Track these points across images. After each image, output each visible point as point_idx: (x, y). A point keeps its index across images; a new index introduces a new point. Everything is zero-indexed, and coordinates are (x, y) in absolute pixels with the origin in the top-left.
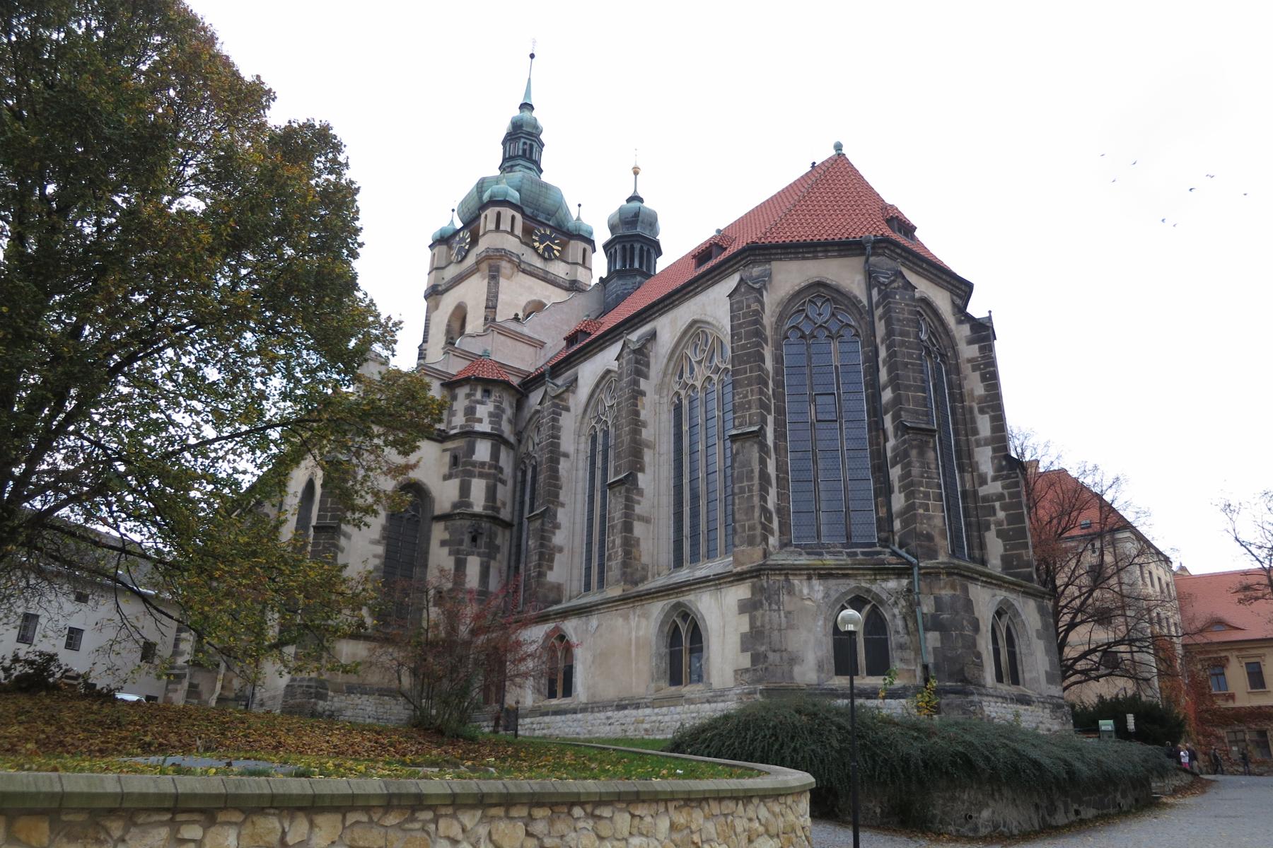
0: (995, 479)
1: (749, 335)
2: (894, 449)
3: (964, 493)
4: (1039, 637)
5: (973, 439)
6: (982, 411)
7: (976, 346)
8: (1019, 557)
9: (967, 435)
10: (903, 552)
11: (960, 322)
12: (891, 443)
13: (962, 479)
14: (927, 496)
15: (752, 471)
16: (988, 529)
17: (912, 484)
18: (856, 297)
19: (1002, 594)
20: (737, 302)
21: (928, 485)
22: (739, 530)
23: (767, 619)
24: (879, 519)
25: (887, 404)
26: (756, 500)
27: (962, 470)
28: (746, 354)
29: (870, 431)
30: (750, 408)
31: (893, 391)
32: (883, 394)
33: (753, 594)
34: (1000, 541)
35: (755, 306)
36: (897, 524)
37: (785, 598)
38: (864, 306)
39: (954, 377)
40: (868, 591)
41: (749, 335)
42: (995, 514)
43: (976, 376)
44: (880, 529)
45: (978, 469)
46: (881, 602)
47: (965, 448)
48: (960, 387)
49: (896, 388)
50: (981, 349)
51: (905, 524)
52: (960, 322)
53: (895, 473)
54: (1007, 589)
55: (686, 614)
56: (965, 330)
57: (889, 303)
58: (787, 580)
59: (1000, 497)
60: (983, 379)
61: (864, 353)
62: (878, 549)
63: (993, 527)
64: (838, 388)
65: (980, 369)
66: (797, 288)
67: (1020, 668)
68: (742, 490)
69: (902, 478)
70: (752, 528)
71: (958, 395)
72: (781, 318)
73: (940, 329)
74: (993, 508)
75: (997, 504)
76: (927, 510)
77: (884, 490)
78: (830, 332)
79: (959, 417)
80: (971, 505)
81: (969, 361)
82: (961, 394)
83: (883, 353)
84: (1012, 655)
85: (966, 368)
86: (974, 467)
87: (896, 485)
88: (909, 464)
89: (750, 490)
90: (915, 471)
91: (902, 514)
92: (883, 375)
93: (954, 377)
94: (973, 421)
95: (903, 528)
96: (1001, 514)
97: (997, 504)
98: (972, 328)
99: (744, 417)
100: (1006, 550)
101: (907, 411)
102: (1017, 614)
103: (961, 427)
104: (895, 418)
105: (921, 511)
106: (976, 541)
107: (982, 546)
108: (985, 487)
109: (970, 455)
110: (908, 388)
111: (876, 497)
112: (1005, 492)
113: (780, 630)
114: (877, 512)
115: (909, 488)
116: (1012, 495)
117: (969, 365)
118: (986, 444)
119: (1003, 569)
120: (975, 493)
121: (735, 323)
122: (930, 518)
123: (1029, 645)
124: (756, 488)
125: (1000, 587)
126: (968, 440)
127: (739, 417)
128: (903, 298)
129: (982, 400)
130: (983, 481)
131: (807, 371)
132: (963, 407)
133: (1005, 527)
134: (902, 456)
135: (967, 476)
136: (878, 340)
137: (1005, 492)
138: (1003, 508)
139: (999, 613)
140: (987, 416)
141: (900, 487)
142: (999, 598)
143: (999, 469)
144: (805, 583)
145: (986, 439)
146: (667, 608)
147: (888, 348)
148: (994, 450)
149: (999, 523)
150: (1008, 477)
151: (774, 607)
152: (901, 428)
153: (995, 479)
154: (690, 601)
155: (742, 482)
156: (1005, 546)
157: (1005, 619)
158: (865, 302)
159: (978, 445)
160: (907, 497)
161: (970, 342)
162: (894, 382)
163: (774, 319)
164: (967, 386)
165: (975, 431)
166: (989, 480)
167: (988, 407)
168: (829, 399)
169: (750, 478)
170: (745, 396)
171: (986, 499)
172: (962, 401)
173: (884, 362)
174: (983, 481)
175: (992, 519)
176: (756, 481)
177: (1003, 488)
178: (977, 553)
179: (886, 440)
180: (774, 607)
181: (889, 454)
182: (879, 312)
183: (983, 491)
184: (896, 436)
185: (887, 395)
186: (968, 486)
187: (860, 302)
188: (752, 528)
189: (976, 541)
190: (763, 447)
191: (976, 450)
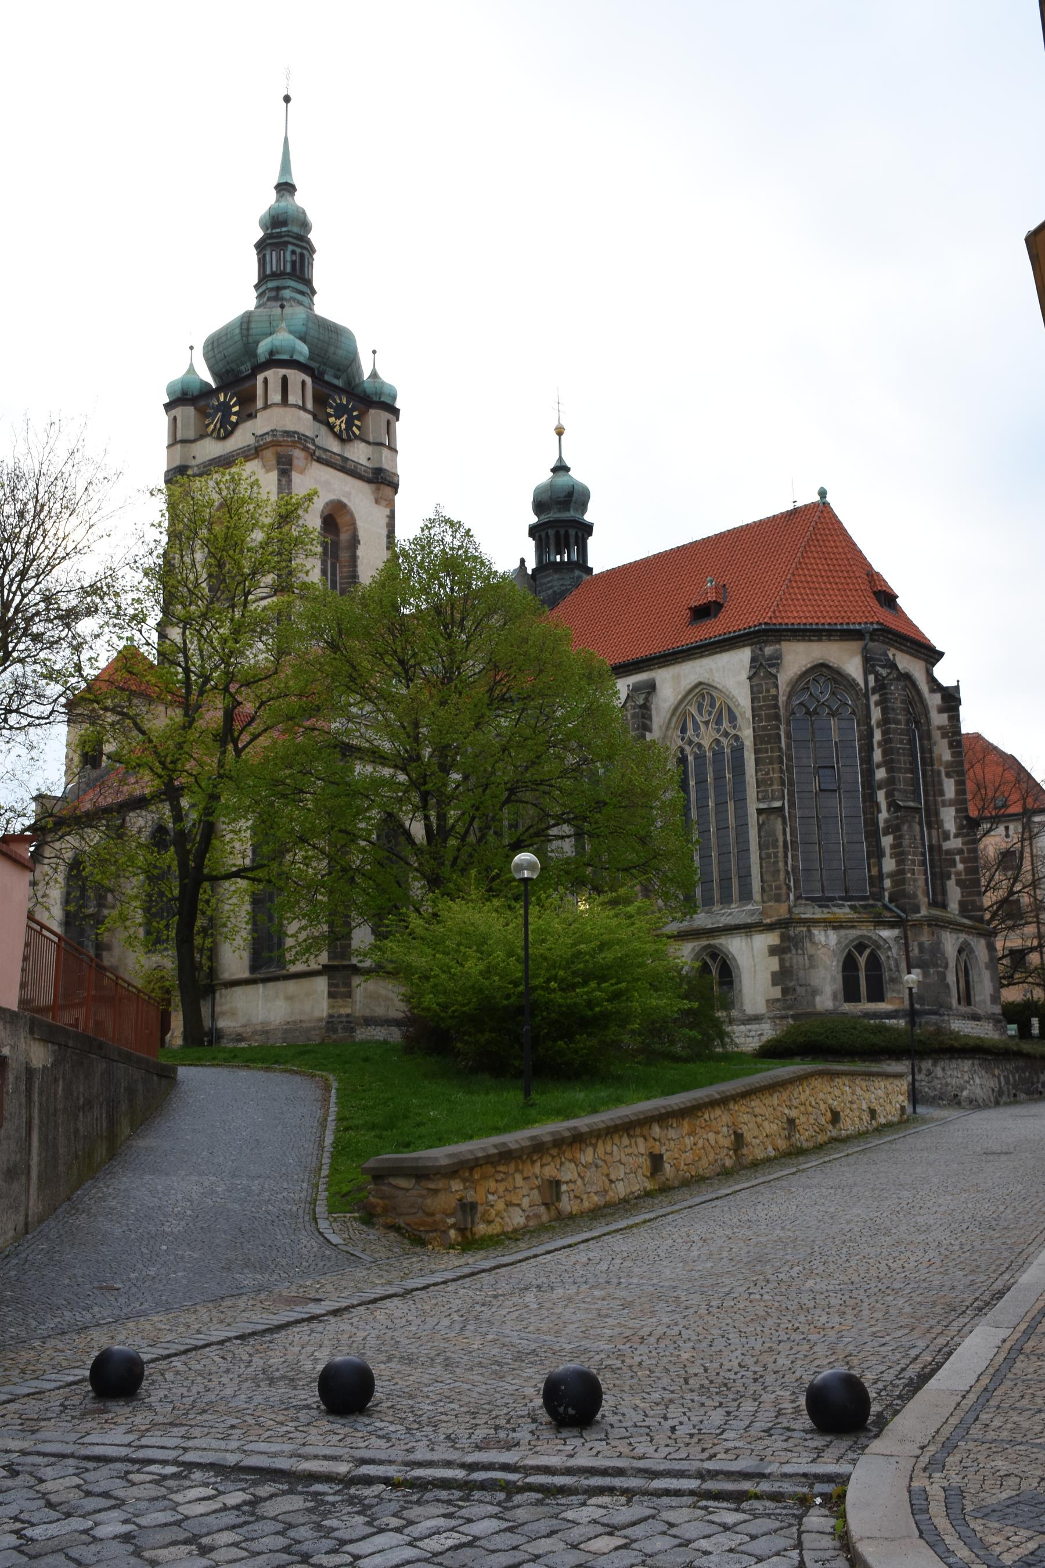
0: (956, 836)
1: (769, 718)
2: (886, 821)
3: (931, 847)
4: (987, 968)
5: (940, 799)
6: (948, 776)
7: (946, 715)
8: (973, 902)
9: (934, 796)
10: (892, 906)
11: (932, 691)
12: (884, 815)
13: (930, 834)
14: (913, 861)
15: (777, 840)
16: (949, 878)
17: (902, 853)
18: (854, 680)
19: (963, 937)
20: (757, 685)
21: (914, 854)
22: (767, 889)
23: (795, 961)
24: (870, 877)
25: (881, 781)
26: (781, 864)
27: (929, 828)
28: (766, 735)
29: (864, 801)
30: (771, 784)
31: (888, 772)
32: (876, 771)
33: (782, 941)
34: (958, 889)
35: (773, 692)
36: (887, 883)
37: (808, 945)
38: (861, 689)
39: (926, 742)
40: (870, 938)
41: (769, 718)
42: (955, 866)
43: (945, 741)
44: (872, 885)
45: (943, 826)
46: (879, 947)
47: (932, 807)
48: (931, 751)
49: (889, 771)
50: (950, 718)
51: (896, 883)
52: (932, 691)
53: (887, 841)
54: (968, 933)
55: (715, 953)
56: (934, 700)
57: (886, 694)
58: (809, 931)
59: (960, 852)
60: (951, 746)
61: (859, 731)
62: (871, 902)
63: (953, 876)
64: (838, 763)
65: (948, 737)
66: (804, 669)
67: (972, 993)
68: (769, 856)
69: (893, 847)
70: (778, 888)
71: (929, 760)
72: (790, 697)
73: (916, 699)
74: (954, 860)
75: (958, 858)
76: (913, 874)
77: (877, 853)
78: (831, 709)
79: (929, 779)
80: (936, 858)
81: (939, 728)
82: (931, 758)
83: (878, 736)
84: (967, 982)
85: (937, 735)
86: (940, 824)
87: (888, 851)
88: (901, 837)
89: (776, 856)
90: (906, 842)
91: (891, 875)
92: (877, 755)
93: (926, 742)
94: (940, 783)
95: (893, 887)
96: (960, 867)
97: (958, 858)
98: (943, 698)
99: (767, 791)
100: (963, 896)
101: (899, 790)
102: (972, 951)
103: (930, 788)
104: (888, 795)
105: (909, 875)
106: (939, 888)
107: (944, 893)
108: (948, 842)
109: (937, 814)
110: (899, 770)
111: (869, 858)
112: (965, 848)
113: (805, 969)
114: (869, 871)
115: (899, 855)
116: (969, 851)
117: (939, 732)
118: (950, 805)
119: (960, 912)
120: (940, 846)
121: (756, 704)
122: (915, 880)
123: (980, 975)
124: (781, 855)
125: (961, 931)
126: (935, 801)
127: (762, 791)
128: (896, 689)
129: (948, 765)
130: (946, 836)
131: (811, 745)
132: (932, 771)
133: (963, 877)
134: (893, 828)
135: (934, 832)
136: (873, 722)
137: (965, 848)
138: (962, 861)
139: (960, 952)
140: (952, 780)
141: (891, 854)
142: (961, 940)
143: (960, 827)
144: (823, 933)
145: (951, 800)
146: (697, 949)
147: (884, 733)
148: (957, 811)
149: (958, 874)
150: (967, 835)
151: (800, 952)
152: (892, 805)
153: (956, 836)
154: (721, 944)
155: (768, 849)
156: (962, 893)
157: (964, 956)
158: (862, 685)
159: (944, 805)
160: (898, 863)
161: (941, 711)
162: (888, 763)
163: (785, 698)
164: (936, 751)
165: (942, 793)
166: (952, 836)
167: (954, 772)
168: (829, 772)
169: (776, 846)
170: (768, 773)
171: (949, 852)
172: (932, 765)
173: (879, 744)
174: (946, 836)
175: (953, 870)
176: (781, 849)
177: (963, 844)
178: (939, 898)
179: (879, 811)
180: (800, 952)
181: (881, 824)
182: (874, 698)
183: (947, 845)
184: (888, 810)
185: (881, 774)
186: (934, 842)
187: (858, 685)
188: (778, 888)
189: (939, 888)
190: (784, 818)
191: (942, 809)
